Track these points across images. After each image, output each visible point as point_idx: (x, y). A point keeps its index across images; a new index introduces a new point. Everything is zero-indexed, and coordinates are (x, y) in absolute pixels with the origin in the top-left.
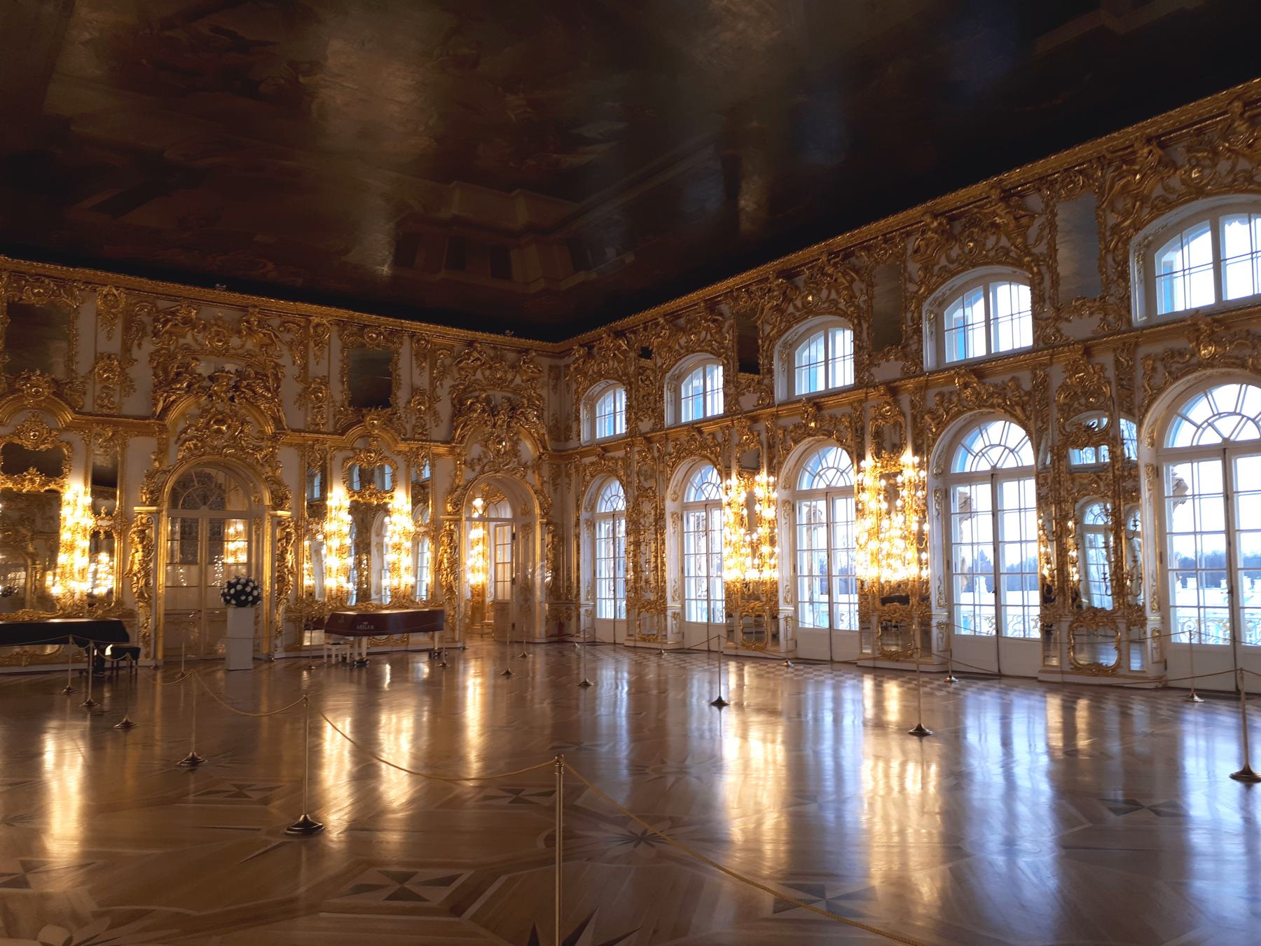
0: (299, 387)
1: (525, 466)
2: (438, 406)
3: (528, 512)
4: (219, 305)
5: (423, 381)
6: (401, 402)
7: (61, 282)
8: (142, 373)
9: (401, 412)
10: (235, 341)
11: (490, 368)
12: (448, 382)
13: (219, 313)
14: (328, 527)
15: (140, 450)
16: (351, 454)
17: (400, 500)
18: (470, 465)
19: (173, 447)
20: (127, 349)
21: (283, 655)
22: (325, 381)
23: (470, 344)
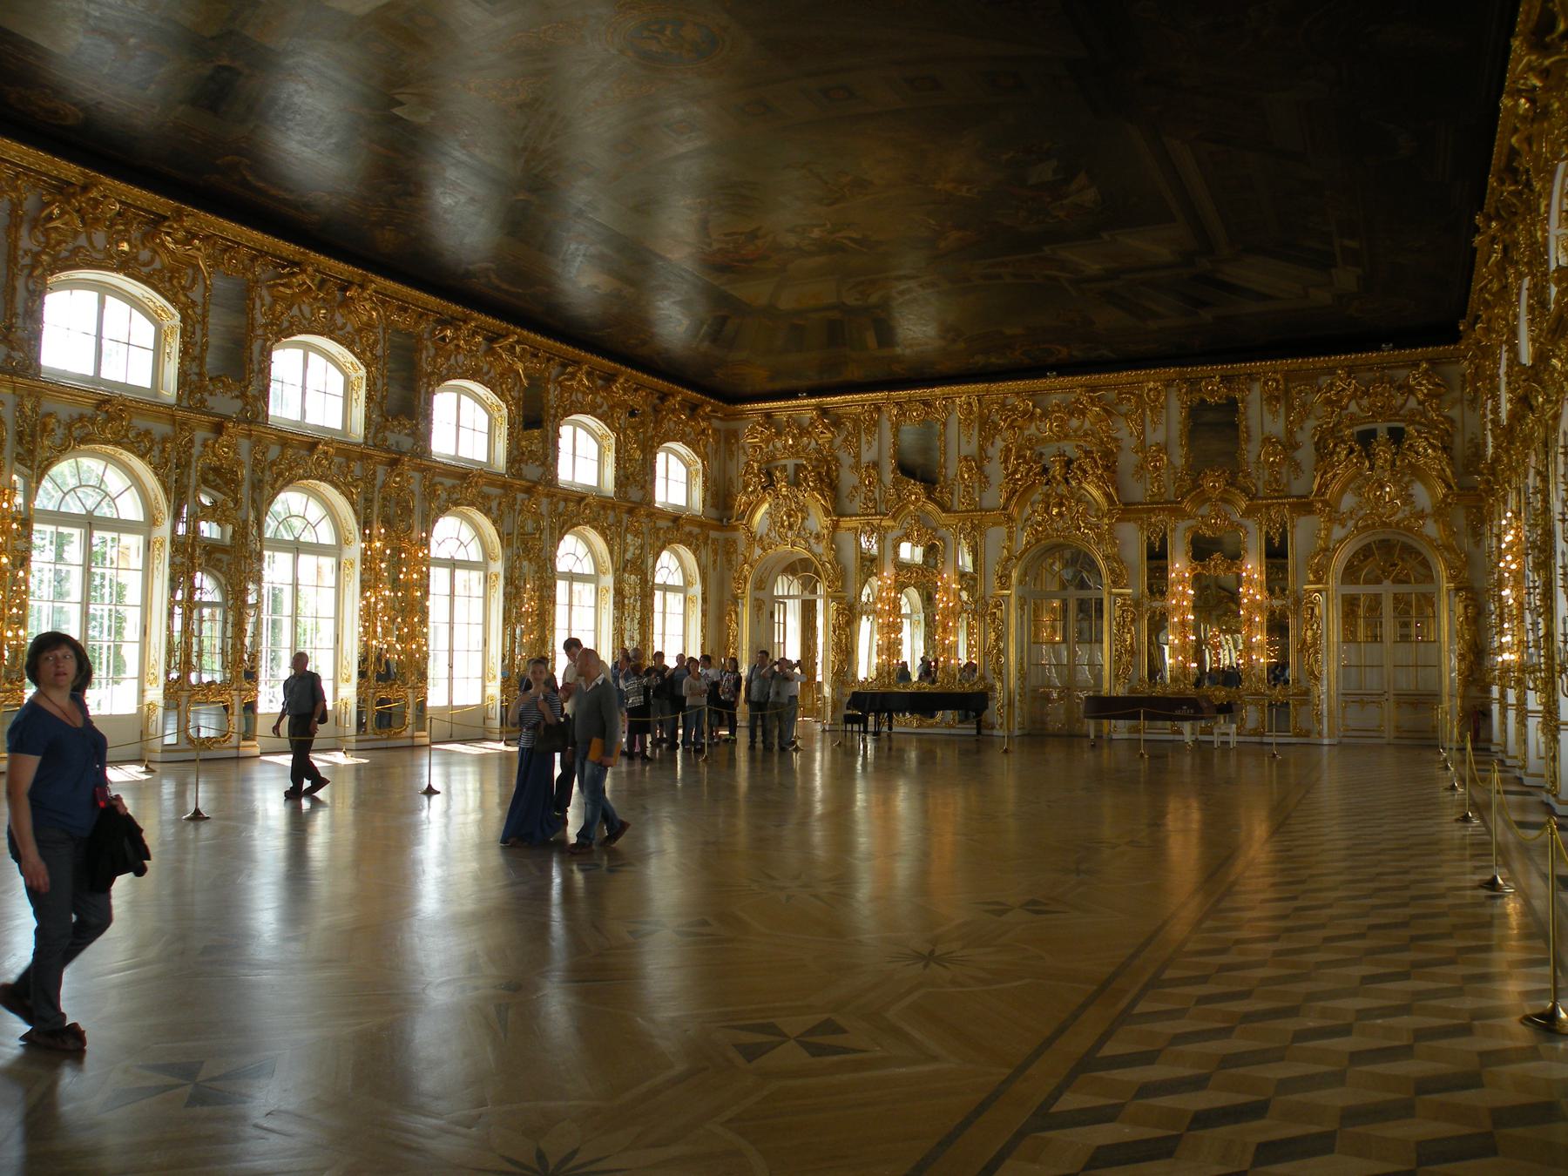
0: (1135, 459)
1: (1421, 515)
5: (1276, 426)
6: (1252, 458)
10: (1075, 423)
11: (1366, 393)
16: (1192, 522)
20: (982, 448)
21: (1126, 736)
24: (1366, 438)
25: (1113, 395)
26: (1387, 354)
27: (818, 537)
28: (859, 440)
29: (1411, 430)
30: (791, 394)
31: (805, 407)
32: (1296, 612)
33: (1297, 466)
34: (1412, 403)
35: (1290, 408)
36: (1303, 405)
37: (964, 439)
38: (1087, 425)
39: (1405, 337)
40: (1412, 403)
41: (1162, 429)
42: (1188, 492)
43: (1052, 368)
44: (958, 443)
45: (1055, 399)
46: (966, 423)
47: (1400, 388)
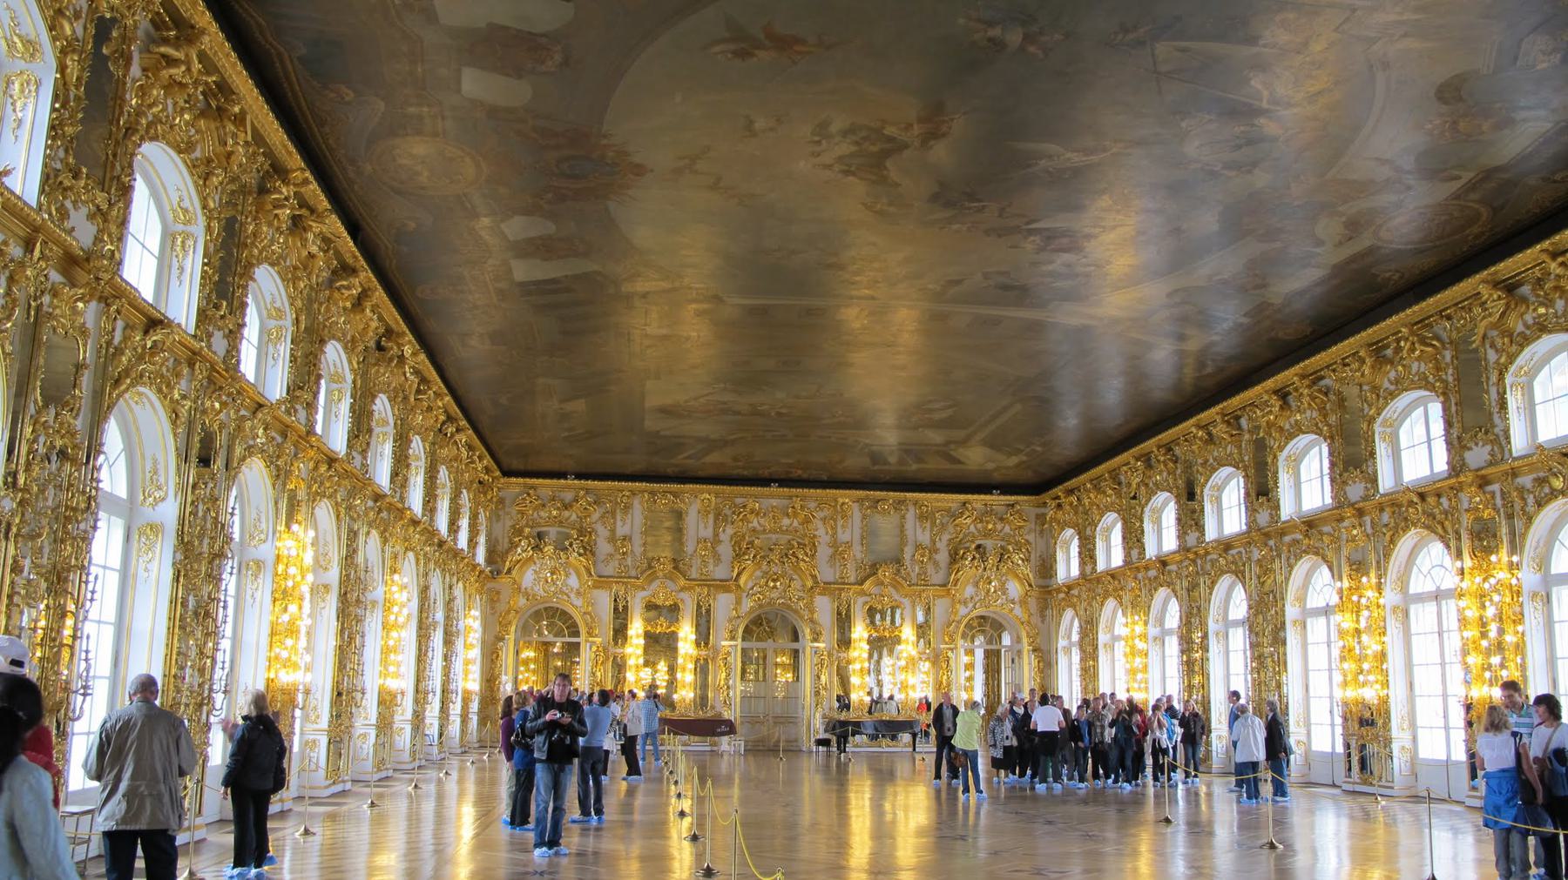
0: (831, 551)
2: (938, 557)
3: (1019, 640)
4: (773, 498)
5: (924, 538)
6: (907, 556)
7: (675, 495)
8: (726, 550)
9: (907, 563)
10: (786, 521)
12: (946, 537)
13: (774, 502)
14: (853, 654)
15: (723, 604)
17: (908, 633)
18: (965, 603)
19: (744, 600)
20: (716, 535)
22: (849, 545)
25: (812, 505)
26: (997, 500)
27: (578, 593)
28: (614, 517)
30: (561, 475)
33: (936, 564)
35: (933, 524)
36: (942, 524)
37: (702, 526)
38: (796, 523)
39: (1008, 488)
40: (1007, 529)
41: (848, 531)
43: (775, 481)
44: (697, 526)
46: (704, 512)
47: (1002, 519)
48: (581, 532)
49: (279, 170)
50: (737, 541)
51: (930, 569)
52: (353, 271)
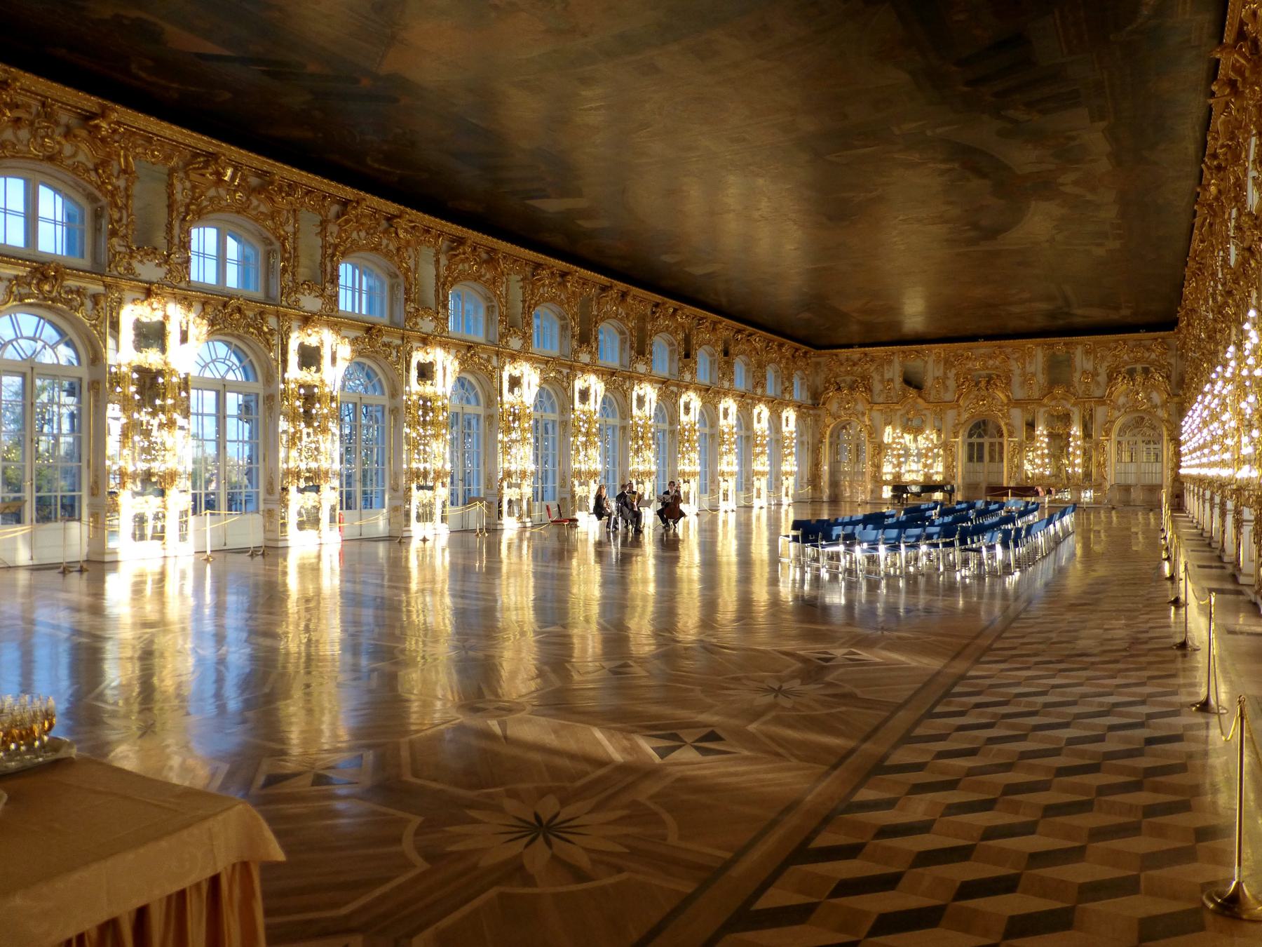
1: (1156, 406)
4: (983, 347)
5: (1089, 366)
8: (951, 383)
10: (991, 362)
12: (1106, 364)
20: (945, 373)
23: (1117, 341)
24: (1131, 373)
25: (1009, 350)
29: (1152, 369)
30: (849, 346)
31: (856, 353)
32: (1096, 449)
33: (1098, 384)
34: (1153, 356)
42: (1044, 396)
45: (982, 351)
46: (937, 362)
47: (1148, 350)
48: (863, 378)
49: (538, 266)
50: (957, 374)
51: (1093, 387)
52: (611, 287)
